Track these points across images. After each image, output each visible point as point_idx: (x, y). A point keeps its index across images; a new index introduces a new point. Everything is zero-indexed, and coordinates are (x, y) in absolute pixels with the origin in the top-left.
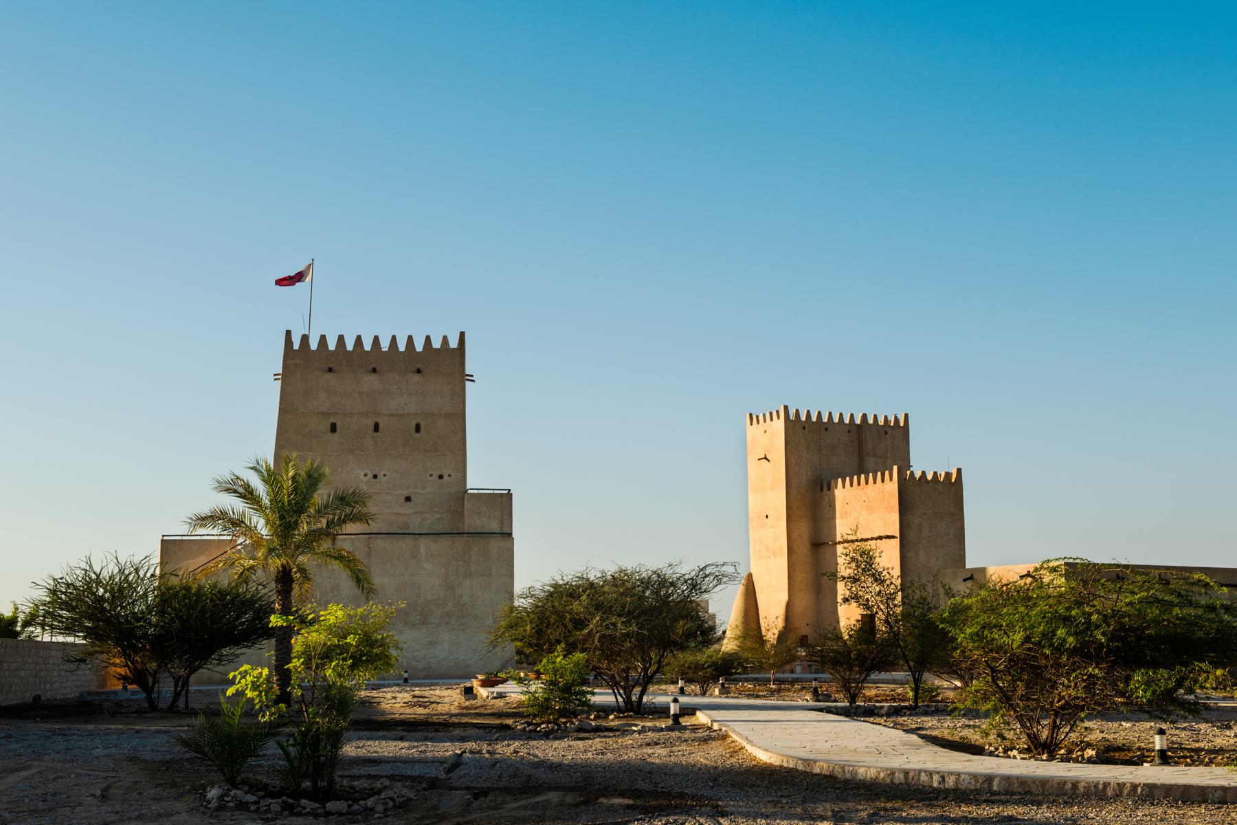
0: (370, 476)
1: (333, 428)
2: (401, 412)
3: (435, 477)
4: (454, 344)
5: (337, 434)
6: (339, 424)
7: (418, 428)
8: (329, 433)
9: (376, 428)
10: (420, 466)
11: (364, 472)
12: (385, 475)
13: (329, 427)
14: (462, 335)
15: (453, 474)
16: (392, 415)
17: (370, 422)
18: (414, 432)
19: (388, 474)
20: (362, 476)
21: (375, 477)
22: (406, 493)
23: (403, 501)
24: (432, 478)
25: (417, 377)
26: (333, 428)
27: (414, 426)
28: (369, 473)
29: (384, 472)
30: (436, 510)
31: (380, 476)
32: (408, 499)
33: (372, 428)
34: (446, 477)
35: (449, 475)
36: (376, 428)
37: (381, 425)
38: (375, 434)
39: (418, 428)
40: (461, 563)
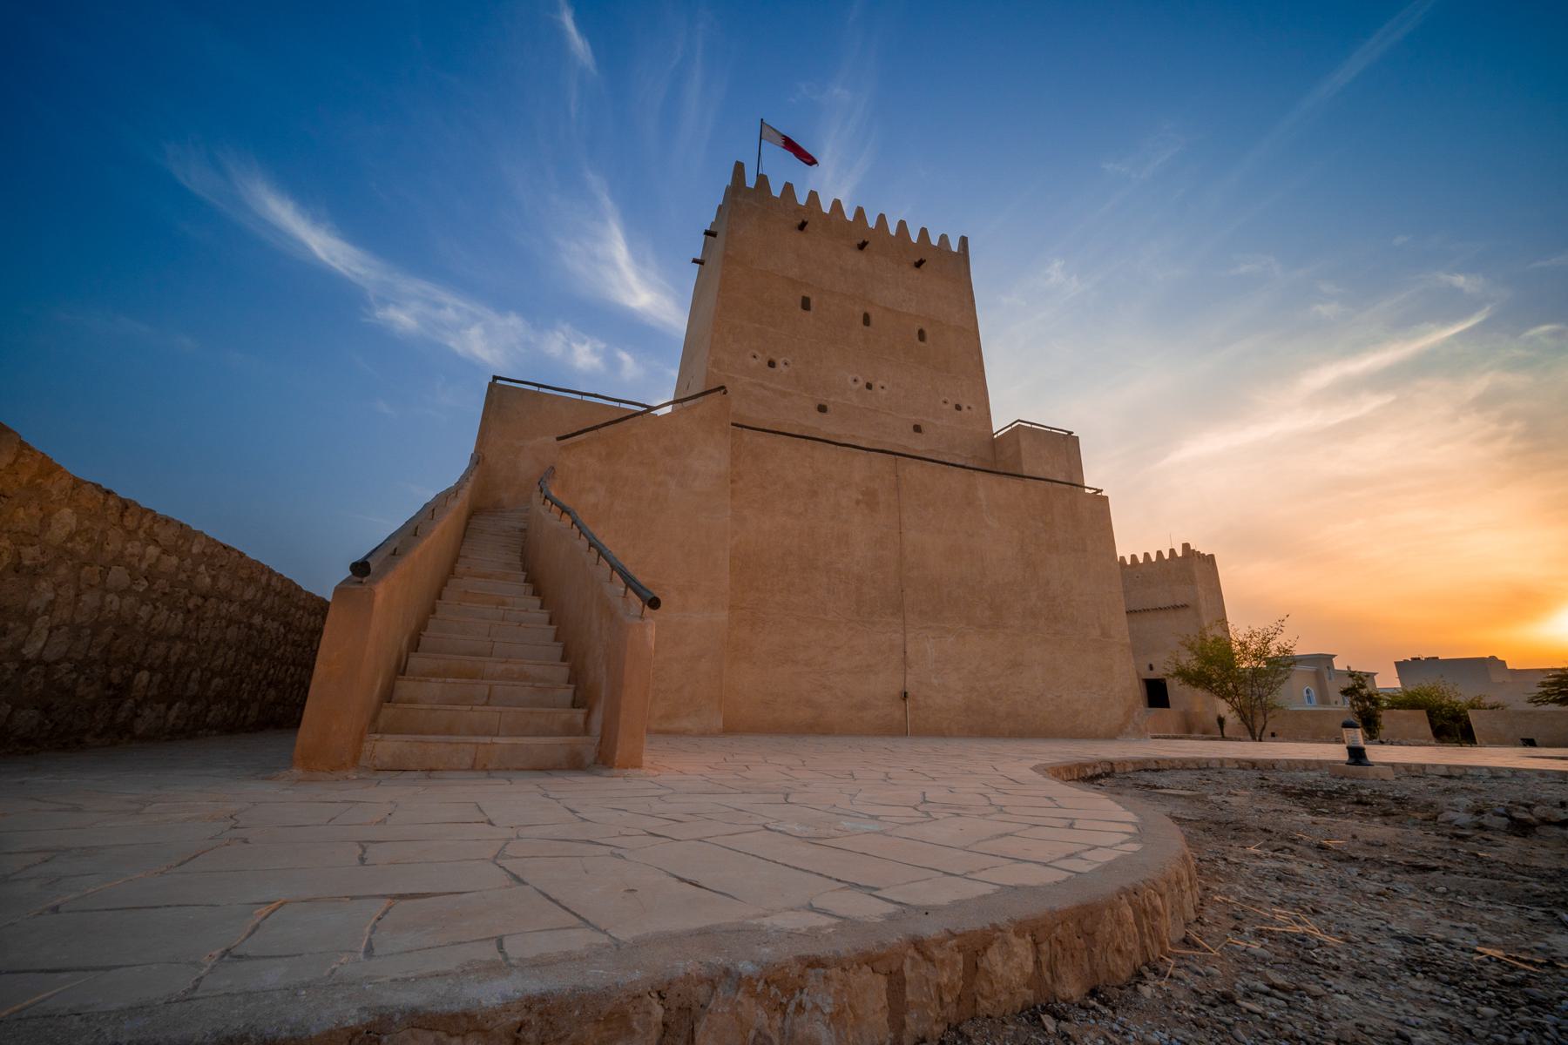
0: (862, 383)
1: (806, 304)
2: (899, 309)
3: (950, 406)
5: (811, 313)
6: (814, 301)
7: (921, 335)
8: (800, 309)
9: (867, 320)
10: (930, 387)
11: (855, 376)
12: (883, 388)
13: (799, 302)
14: (964, 241)
15: (972, 406)
16: (887, 309)
17: (859, 311)
18: (917, 338)
19: (887, 387)
20: (850, 381)
21: (869, 386)
22: (915, 419)
23: (911, 429)
24: (945, 407)
25: (915, 273)
26: (806, 304)
27: (917, 332)
28: (860, 378)
29: (880, 383)
30: (957, 452)
31: (877, 385)
32: (917, 429)
33: (861, 319)
34: (964, 408)
36: (867, 320)
37: (873, 319)
38: (865, 328)
39: (921, 335)
40: (1041, 525)
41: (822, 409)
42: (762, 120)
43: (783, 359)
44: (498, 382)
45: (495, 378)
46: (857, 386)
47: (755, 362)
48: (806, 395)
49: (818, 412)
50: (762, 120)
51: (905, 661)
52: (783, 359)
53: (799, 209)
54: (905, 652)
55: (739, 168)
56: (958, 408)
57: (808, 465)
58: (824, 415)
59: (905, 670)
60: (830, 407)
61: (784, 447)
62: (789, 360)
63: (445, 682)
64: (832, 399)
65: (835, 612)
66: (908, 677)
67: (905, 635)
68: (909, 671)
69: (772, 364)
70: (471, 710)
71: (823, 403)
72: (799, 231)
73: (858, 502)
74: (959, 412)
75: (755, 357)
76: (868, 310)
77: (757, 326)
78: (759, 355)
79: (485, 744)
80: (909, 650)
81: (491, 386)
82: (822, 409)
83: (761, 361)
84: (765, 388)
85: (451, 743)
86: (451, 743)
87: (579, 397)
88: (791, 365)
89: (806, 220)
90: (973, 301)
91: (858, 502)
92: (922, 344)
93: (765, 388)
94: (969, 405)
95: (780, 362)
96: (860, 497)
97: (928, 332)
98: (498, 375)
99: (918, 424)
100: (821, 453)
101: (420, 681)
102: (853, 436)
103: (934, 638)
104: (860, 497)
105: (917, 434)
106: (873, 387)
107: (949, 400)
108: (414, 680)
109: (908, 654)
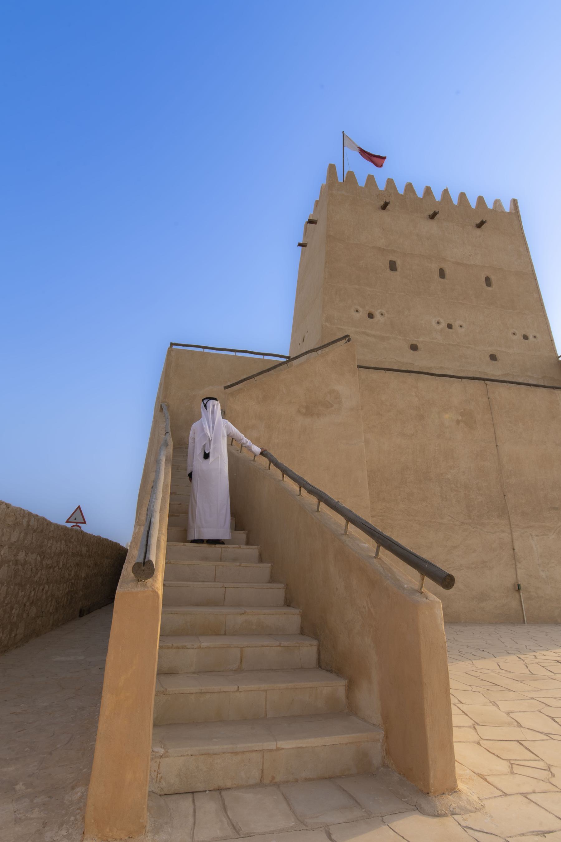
0: (444, 325)
1: (393, 266)
3: (519, 337)
4: (507, 208)
6: (399, 263)
7: (488, 281)
8: (388, 270)
9: (442, 274)
12: (461, 326)
13: (388, 266)
15: (538, 335)
17: (435, 267)
18: (484, 285)
19: (464, 325)
21: (450, 326)
22: (491, 350)
23: (488, 359)
24: (515, 337)
25: (478, 232)
26: (393, 266)
27: (484, 279)
28: (442, 321)
29: (458, 323)
31: (456, 325)
34: (531, 337)
35: (535, 337)
36: (442, 274)
37: (447, 272)
39: (488, 281)
41: (414, 348)
42: (343, 132)
43: (379, 311)
44: (174, 347)
45: (172, 344)
46: (441, 326)
47: (358, 315)
48: (400, 337)
49: (412, 351)
50: (343, 132)
51: (514, 557)
52: (379, 311)
53: (380, 194)
54: (514, 549)
55: (332, 168)
56: (525, 337)
57: (414, 394)
58: (416, 353)
59: (516, 566)
60: (420, 346)
61: (393, 379)
62: (384, 311)
63: (200, 647)
64: (421, 339)
65: (449, 516)
66: (519, 571)
67: (511, 534)
68: (519, 565)
69: (371, 316)
70: (238, 690)
71: (414, 343)
72: (383, 211)
73: (458, 422)
74: (526, 341)
75: (357, 311)
76: (443, 266)
77: (357, 287)
78: (360, 309)
79: (271, 750)
80: (516, 547)
81: (170, 351)
82: (414, 348)
83: (362, 314)
84: (368, 335)
85: (237, 753)
86: (237, 753)
87: (233, 354)
88: (386, 315)
89: (387, 201)
90: (527, 250)
91: (458, 422)
92: (489, 289)
93: (368, 335)
94: (535, 334)
95: (377, 314)
96: (460, 418)
97: (493, 278)
98: (173, 342)
99: (493, 353)
100: (425, 383)
101: (178, 648)
102: (441, 368)
103: (537, 536)
104: (460, 418)
105: (494, 362)
106: (453, 327)
107: (517, 332)
108: (172, 647)
109: (515, 550)
